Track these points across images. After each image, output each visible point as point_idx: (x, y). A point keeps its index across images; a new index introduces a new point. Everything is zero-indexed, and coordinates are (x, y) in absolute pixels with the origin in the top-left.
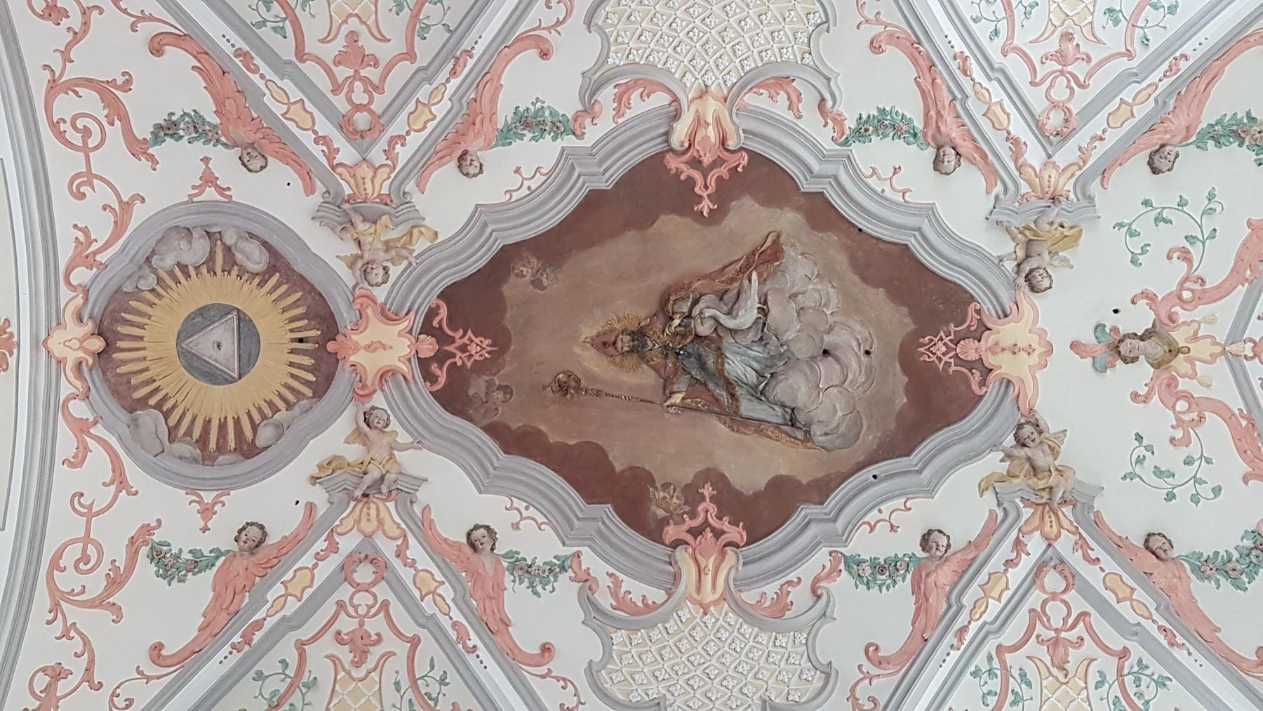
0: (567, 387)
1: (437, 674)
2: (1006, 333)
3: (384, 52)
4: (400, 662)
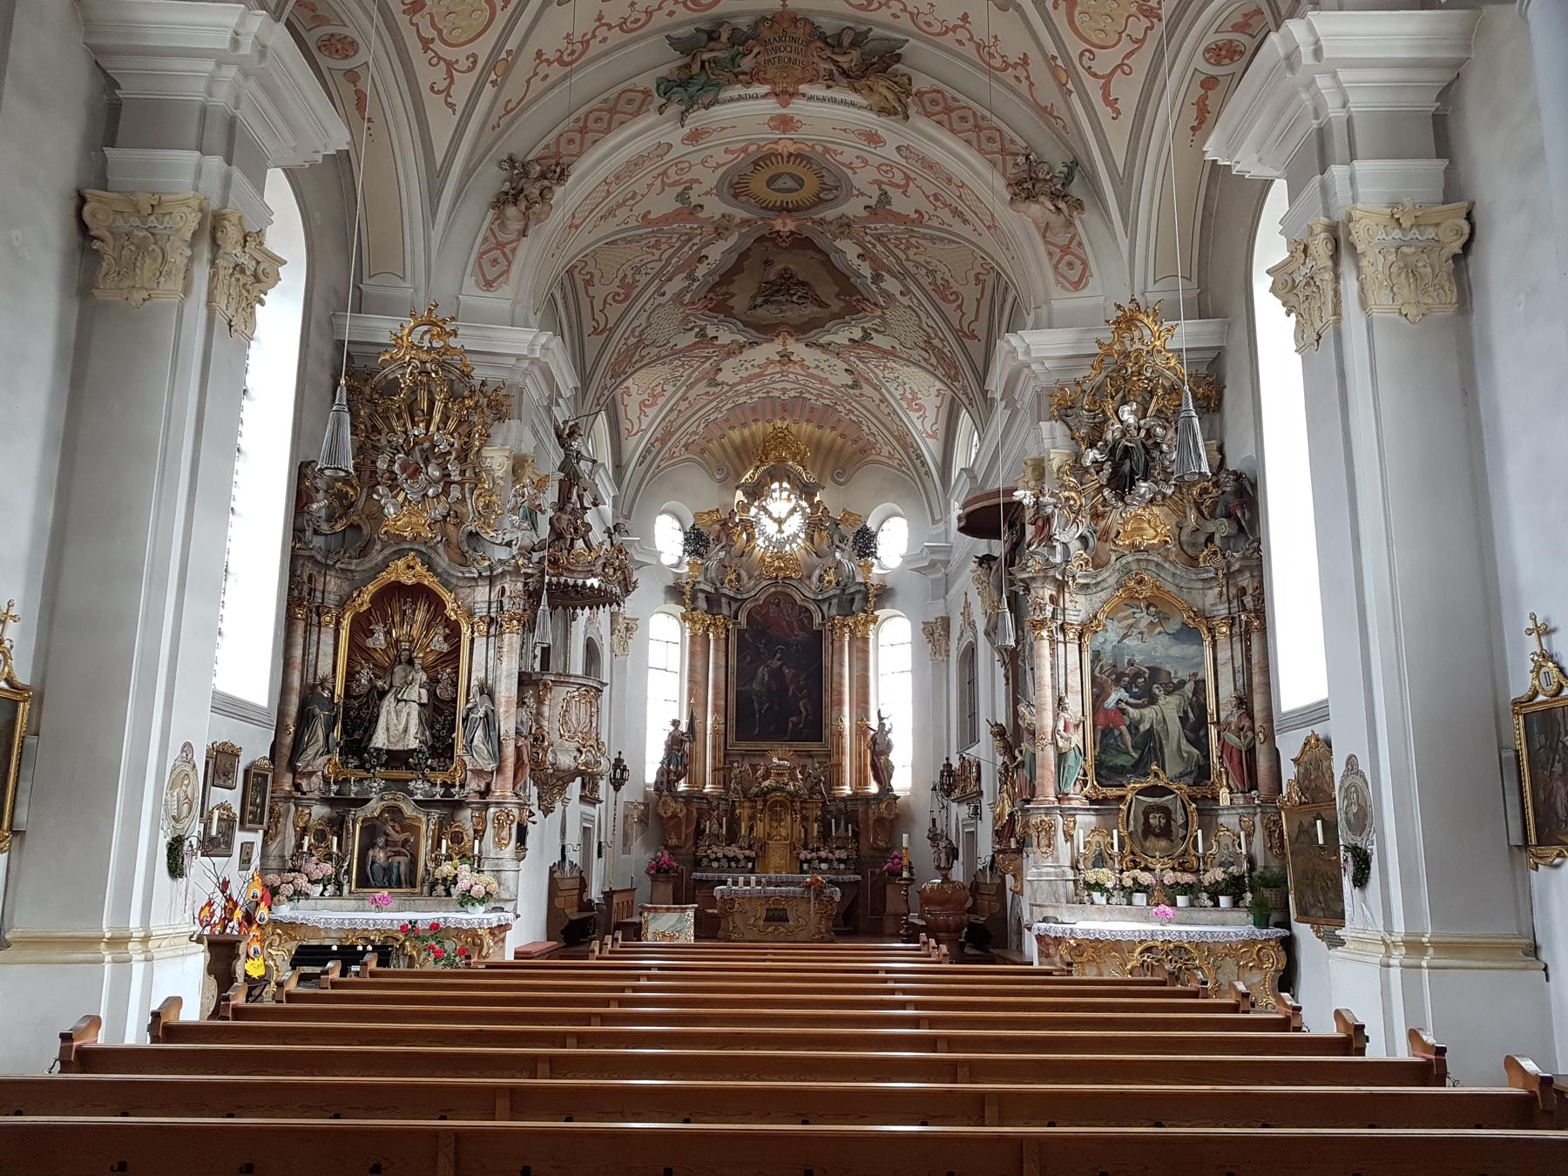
0: (768, 263)
2: (790, 341)
3: (911, 252)
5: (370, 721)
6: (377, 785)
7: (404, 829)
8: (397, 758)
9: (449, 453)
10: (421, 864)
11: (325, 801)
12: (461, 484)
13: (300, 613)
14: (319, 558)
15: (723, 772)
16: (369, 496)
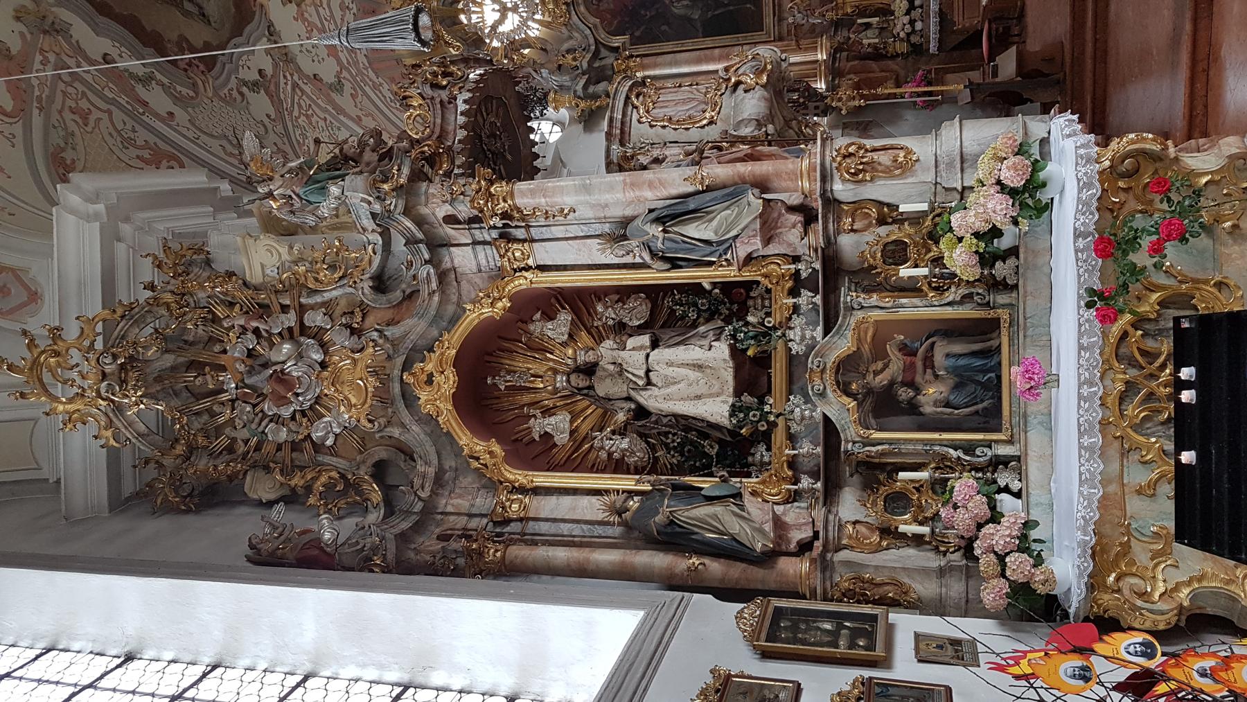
1: (129, 127)
4: (105, 122)
5: (687, 429)
6: (798, 408)
7: (879, 353)
8: (751, 375)
9: (256, 331)
10: (949, 312)
11: (830, 496)
12: (302, 310)
13: (493, 553)
14: (405, 525)
15: (799, 37)
16: (332, 451)
